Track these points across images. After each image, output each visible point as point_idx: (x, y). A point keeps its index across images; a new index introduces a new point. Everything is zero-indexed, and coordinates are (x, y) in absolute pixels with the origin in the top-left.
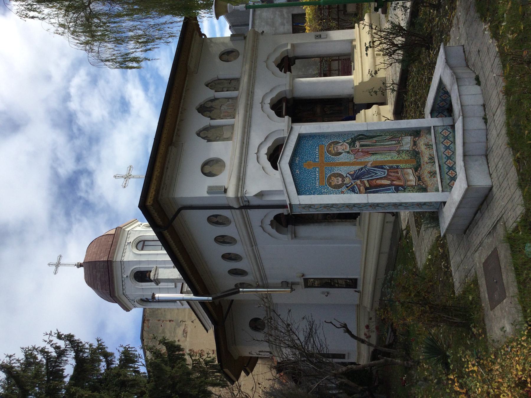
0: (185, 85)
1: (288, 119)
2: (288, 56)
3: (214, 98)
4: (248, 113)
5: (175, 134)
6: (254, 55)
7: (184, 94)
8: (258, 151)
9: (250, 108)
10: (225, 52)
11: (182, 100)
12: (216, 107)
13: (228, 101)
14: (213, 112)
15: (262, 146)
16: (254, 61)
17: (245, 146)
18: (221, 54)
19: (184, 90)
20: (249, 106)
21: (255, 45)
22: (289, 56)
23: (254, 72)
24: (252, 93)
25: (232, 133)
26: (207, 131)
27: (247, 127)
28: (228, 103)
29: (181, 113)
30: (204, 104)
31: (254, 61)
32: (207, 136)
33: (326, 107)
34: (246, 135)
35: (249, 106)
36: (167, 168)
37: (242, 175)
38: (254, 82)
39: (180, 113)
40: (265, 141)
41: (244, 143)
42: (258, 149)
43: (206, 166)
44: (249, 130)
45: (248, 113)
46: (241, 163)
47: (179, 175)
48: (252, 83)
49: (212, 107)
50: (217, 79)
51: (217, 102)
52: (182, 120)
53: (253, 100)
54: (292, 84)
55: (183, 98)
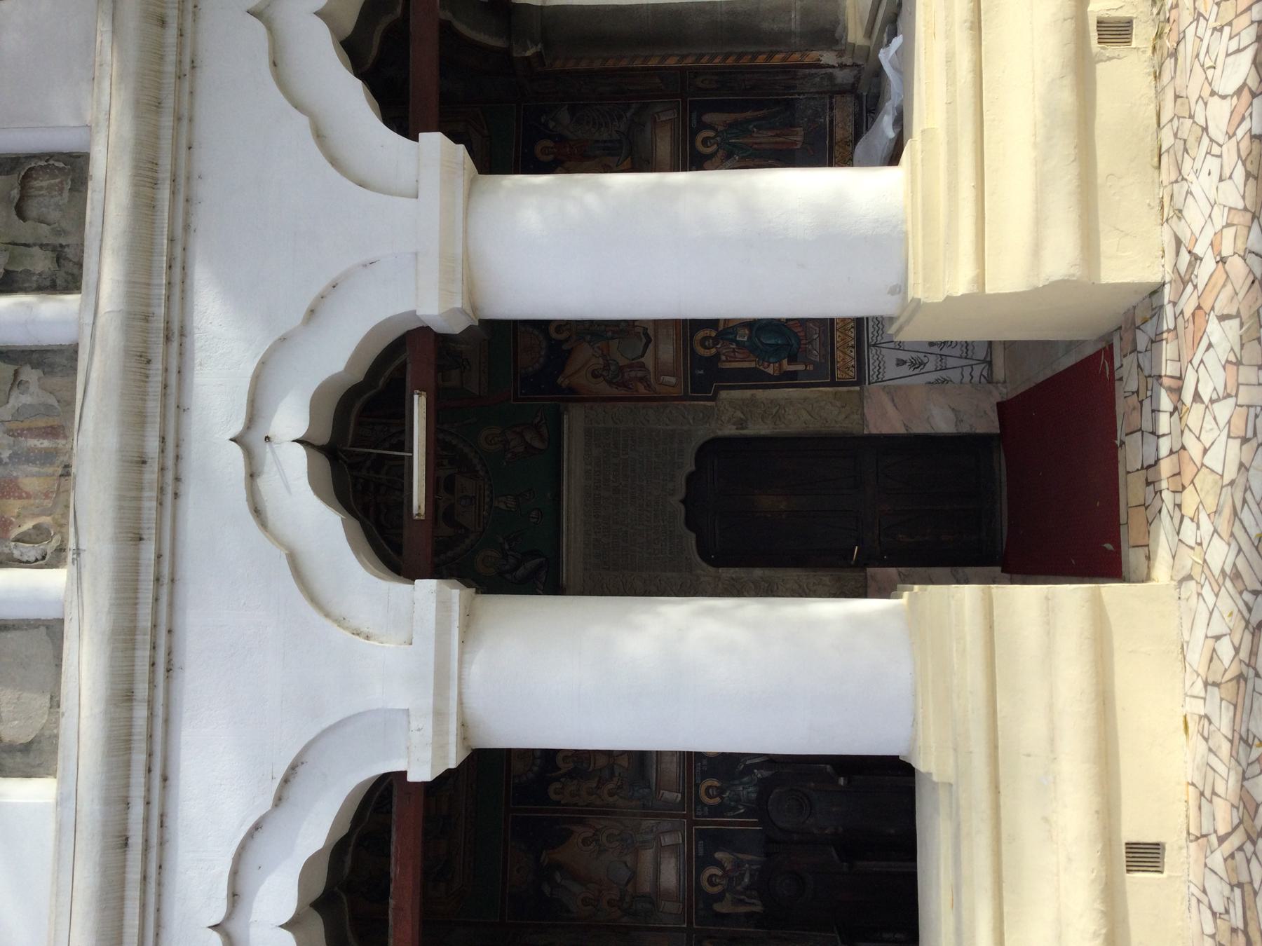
1: (443, 606)
8: (234, 896)
9: (162, 490)
13: (16, 382)
15: (260, 837)
16: (172, 14)
17: (134, 875)
20: (151, 474)
23: (179, 119)
24: (168, 339)
25: (55, 703)
27: (142, 689)
28: (20, 399)
33: (709, 127)
34: (139, 758)
35: (151, 474)
38: (187, 227)
40: (279, 800)
41: (125, 843)
42: (235, 874)
44: (160, 711)
48: (172, 240)
53: (181, 409)
54: (459, 250)
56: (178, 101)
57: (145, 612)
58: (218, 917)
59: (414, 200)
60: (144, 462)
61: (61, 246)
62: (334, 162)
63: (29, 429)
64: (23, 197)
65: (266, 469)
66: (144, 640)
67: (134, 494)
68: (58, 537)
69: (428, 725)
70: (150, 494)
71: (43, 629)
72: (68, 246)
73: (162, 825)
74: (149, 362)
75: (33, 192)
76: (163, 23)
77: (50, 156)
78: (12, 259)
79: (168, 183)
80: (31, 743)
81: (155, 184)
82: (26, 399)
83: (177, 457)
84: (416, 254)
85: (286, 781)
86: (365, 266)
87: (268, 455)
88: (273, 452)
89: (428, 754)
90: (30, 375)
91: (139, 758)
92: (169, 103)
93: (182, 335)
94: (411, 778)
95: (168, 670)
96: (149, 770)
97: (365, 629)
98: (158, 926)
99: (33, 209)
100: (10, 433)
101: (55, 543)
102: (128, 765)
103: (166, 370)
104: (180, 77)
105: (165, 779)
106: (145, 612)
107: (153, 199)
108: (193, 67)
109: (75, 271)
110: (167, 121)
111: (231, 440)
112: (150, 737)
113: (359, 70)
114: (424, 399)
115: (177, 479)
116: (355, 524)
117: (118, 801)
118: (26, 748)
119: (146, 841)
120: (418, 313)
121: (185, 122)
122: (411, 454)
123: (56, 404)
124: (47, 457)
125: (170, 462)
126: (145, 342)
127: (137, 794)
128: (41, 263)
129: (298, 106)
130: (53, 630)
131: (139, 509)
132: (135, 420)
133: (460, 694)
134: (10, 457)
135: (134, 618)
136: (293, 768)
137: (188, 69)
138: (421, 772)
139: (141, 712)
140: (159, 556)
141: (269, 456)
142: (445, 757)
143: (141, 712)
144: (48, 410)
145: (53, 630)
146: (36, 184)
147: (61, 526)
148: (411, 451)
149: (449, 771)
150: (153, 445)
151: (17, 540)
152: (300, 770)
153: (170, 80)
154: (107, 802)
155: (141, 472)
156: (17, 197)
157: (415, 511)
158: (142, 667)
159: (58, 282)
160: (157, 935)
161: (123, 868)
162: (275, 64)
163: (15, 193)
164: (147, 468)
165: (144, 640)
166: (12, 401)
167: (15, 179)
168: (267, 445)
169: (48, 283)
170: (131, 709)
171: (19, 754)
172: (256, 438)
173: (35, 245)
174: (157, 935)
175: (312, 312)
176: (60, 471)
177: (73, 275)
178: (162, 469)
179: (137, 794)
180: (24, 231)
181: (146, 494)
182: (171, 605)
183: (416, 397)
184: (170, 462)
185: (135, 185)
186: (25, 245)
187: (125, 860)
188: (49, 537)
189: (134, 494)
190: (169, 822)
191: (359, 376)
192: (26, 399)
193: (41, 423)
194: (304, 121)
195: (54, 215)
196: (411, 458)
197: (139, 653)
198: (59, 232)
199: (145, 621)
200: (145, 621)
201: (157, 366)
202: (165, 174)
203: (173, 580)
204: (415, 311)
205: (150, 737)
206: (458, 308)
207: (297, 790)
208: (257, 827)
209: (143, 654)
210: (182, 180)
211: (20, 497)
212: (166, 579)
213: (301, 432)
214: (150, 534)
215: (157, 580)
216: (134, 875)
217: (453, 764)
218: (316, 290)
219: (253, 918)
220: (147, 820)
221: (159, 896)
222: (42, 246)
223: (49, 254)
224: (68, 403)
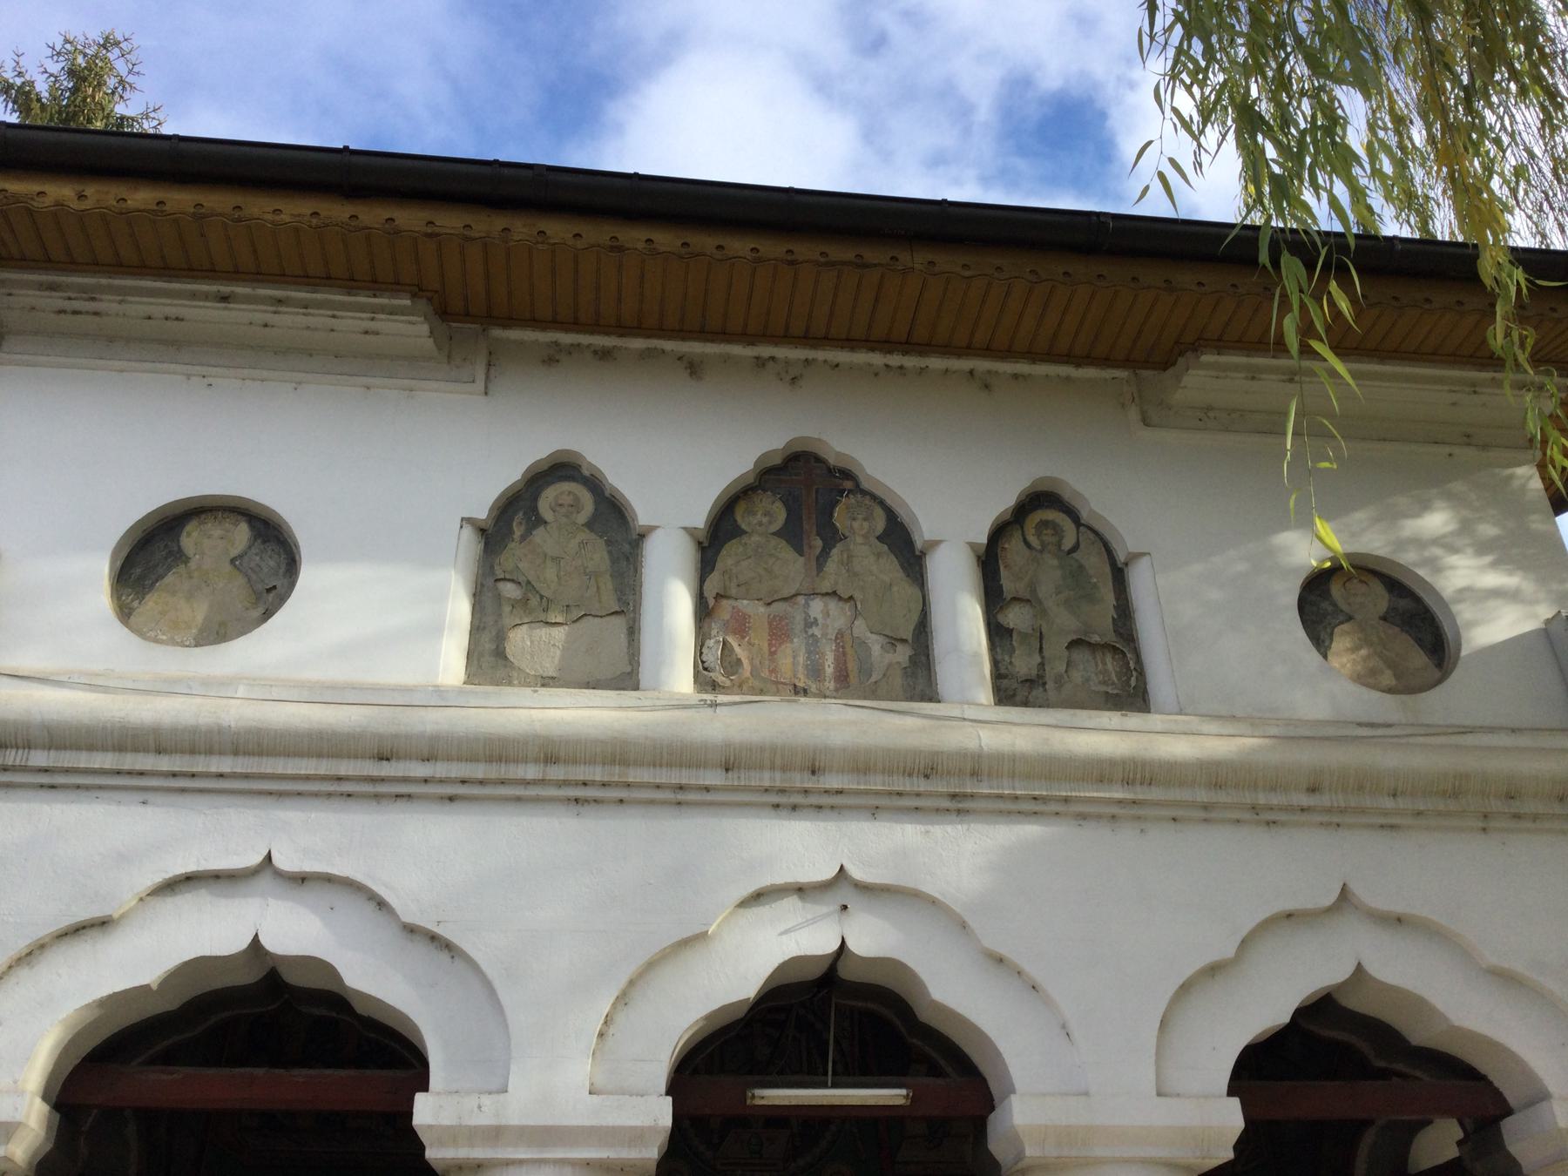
0: (1023, 368)
1: (635, 1136)
2: (1509, 1112)
3: (919, 544)
4: (714, 778)
5: (567, 338)
6: (1402, 803)
7: (936, 363)
8: (302, 879)
9: (782, 791)
10: (1417, 600)
11: (877, 359)
12: (831, 566)
13: (894, 641)
14: (787, 552)
15: (370, 907)
16: (1324, 800)
17: (345, 768)
18: (1371, 566)
19: (982, 365)
20: (800, 780)
21: (1529, 807)
22: (1507, 1125)
23: (1206, 807)
24: (954, 796)
25: (547, 682)
26: (590, 525)
27: (557, 772)
28: (876, 645)
29: (760, 363)
30: (864, 493)
31: (1324, 800)
32: (541, 522)
34: (479, 771)
35: (800, 780)
36: (225, 299)
37: (39, 758)
38: (1083, 817)
39: (766, 351)
40: (411, 930)
41: (383, 757)
42: (328, 879)
43: (242, 533)
44: (532, 791)
45: (714, 778)
46: (159, 751)
47: (189, 376)
48: (1066, 800)
49: (831, 536)
50: (1121, 557)
51: (888, 568)
52: (694, 368)
53: (875, 812)
54: (1099, 1152)
55: (895, 360)
56: (1226, 807)
57: (644, 775)
58: (280, 862)
59: (1155, 1093)
60: (813, 773)
61: (1044, 684)
62: (1185, 989)
63: (844, 654)
64: (1093, 647)
65: (808, 906)
66: (615, 774)
67: (778, 762)
68: (728, 683)
69: (485, 1119)
70: (778, 780)
71: (629, 669)
72: (1045, 690)
73: (398, 796)
74: (927, 776)
75: (1099, 655)
76: (1313, 790)
77: (1141, 673)
78: (1024, 637)
79: (1129, 796)
80: (506, 658)
81: (1128, 782)
82: (876, 649)
83: (820, 807)
84: (1086, 1094)
85: (433, 938)
86: (1064, 1027)
87: (827, 907)
88: (828, 915)
89: (447, 1119)
90: (903, 654)
91: (479, 771)
92: (1222, 797)
93: (959, 812)
94: (419, 1098)
95: (577, 800)
96: (463, 782)
97: (612, 1030)
98: (281, 795)
99: (1080, 655)
100: (840, 635)
101: (721, 679)
102: (473, 758)
103: (918, 795)
104: (1254, 808)
105: (451, 799)
106: (644, 775)
107: (1111, 781)
108: (1268, 823)
109: (1018, 698)
110: (1203, 796)
111: (842, 866)
112: (502, 782)
113: (1302, 1013)
114: (901, 1102)
115: (794, 808)
116: (741, 1014)
117: (432, 749)
118: (500, 654)
119: (382, 780)
120: (1013, 1097)
121: (1202, 814)
122: (830, 1084)
123: (873, 679)
124: (816, 672)
125: (813, 800)
126: (949, 773)
127: (439, 769)
128: (1023, 664)
129: (1244, 944)
130: (627, 679)
131: (761, 768)
132: (862, 763)
133: (521, 1162)
134: (813, 635)
135: (639, 763)
136: (447, 946)
137: (1266, 818)
138: (426, 1111)
139: (532, 772)
140: (707, 789)
141: (824, 909)
142: (441, 1144)
143: (532, 772)
144: (865, 670)
145: (627, 679)
146: (1109, 659)
147: (740, 686)
148: (835, 1086)
149: (422, 1148)
150: (833, 782)
151: (725, 643)
152: (444, 957)
153: (1248, 798)
154: (435, 739)
155: (802, 769)
156: (1092, 641)
157: (759, 1092)
158: (581, 773)
159: (1005, 682)
160: (270, 793)
161: (354, 755)
162: (1289, 916)
163: (1096, 639)
164: (807, 775)
165: (615, 774)
166: (874, 637)
167: (1111, 638)
168: (838, 908)
169: (1003, 671)
170: (536, 761)
171: (494, 647)
172: (844, 895)
173: (1043, 658)
174: (270, 793)
175: (1000, 960)
176: (801, 684)
177: (1014, 695)
178: (806, 792)
179: (439, 769)
180: (1056, 647)
181: (778, 775)
182: (652, 802)
183: (903, 1092)
184: (813, 800)
185: (1124, 762)
186: (1041, 648)
187: (363, 757)
188: (728, 674)
189: (778, 762)
190: (400, 804)
191: (924, 1016)
192: (876, 649)
193: (852, 666)
194: (1229, 951)
195: (1077, 676)
196: (824, 1086)
197: (599, 769)
198: (1059, 681)
199: (635, 775)
200: (635, 775)
201: (923, 786)
202: (1140, 793)
203: (679, 803)
204: (1013, 1091)
205: (502, 782)
206: (1022, 1151)
207: (420, 952)
208: (381, 904)
209: (598, 774)
210: (1135, 811)
211: (770, 645)
212: (681, 797)
213: (855, 946)
214: (733, 779)
215: (681, 788)
216: (345, 768)
217: (431, 1154)
218: (1027, 967)
219: (271, 901)
220: (406, 780)
221: (316, 795)
222: (1042, 665)
223: (1034, 672)
224: (873, 693)
